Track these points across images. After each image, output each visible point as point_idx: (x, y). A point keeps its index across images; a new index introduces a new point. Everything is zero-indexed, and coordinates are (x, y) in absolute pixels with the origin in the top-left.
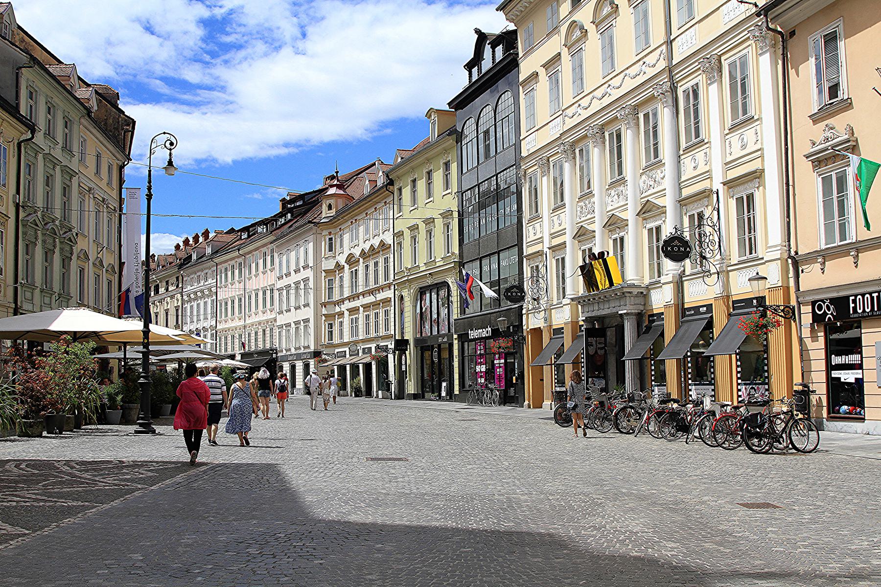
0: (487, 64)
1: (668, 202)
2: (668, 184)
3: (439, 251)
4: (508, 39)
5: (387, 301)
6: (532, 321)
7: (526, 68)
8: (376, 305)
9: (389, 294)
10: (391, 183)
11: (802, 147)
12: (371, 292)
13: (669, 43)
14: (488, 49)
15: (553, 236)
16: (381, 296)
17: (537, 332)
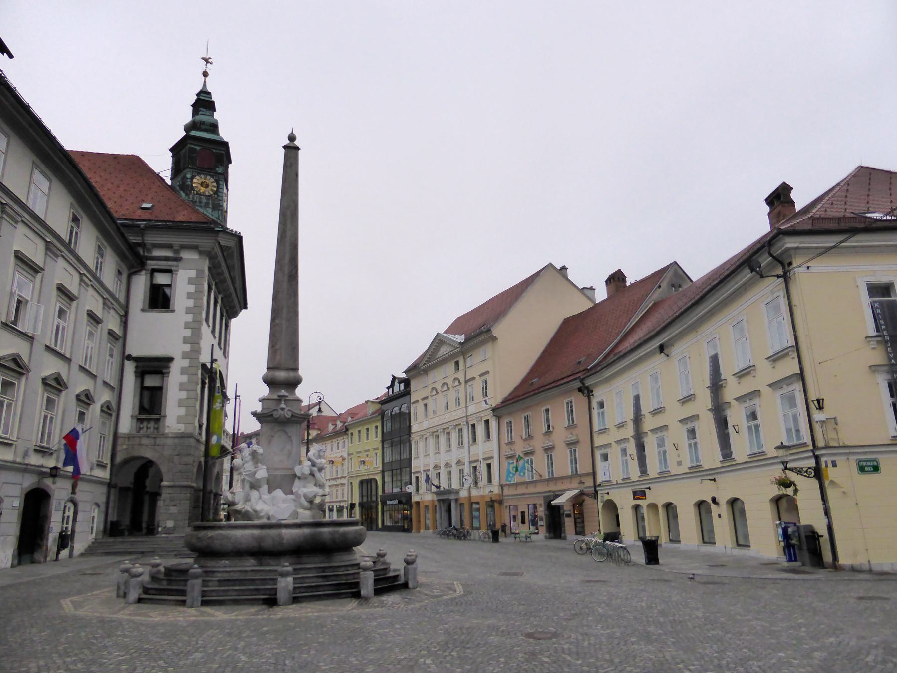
0: (396, 389)
1: (467, 462)
2: (466, 455)
3: (373, 467)
4: (406, 382)
5: (343, 484)
6: (415, 498)
7: (414, 397)
8: (337, 485)
9: (345, 481)
10: (347, 430)
11: (503, 453)
12: (335, 479)
13: (467, 407)
14: (396, 384)
15: (424, 466)
16: (340, 481)
17: (418, 503)
